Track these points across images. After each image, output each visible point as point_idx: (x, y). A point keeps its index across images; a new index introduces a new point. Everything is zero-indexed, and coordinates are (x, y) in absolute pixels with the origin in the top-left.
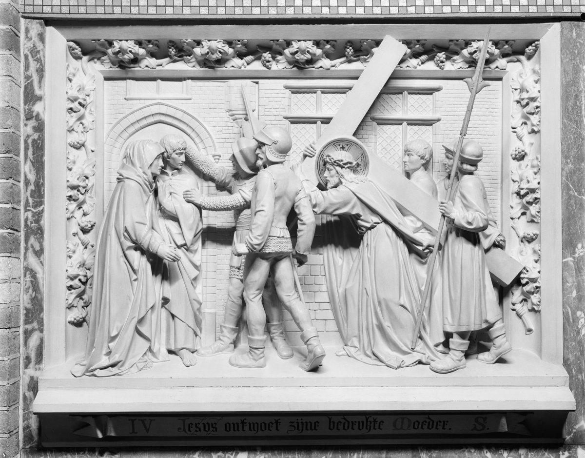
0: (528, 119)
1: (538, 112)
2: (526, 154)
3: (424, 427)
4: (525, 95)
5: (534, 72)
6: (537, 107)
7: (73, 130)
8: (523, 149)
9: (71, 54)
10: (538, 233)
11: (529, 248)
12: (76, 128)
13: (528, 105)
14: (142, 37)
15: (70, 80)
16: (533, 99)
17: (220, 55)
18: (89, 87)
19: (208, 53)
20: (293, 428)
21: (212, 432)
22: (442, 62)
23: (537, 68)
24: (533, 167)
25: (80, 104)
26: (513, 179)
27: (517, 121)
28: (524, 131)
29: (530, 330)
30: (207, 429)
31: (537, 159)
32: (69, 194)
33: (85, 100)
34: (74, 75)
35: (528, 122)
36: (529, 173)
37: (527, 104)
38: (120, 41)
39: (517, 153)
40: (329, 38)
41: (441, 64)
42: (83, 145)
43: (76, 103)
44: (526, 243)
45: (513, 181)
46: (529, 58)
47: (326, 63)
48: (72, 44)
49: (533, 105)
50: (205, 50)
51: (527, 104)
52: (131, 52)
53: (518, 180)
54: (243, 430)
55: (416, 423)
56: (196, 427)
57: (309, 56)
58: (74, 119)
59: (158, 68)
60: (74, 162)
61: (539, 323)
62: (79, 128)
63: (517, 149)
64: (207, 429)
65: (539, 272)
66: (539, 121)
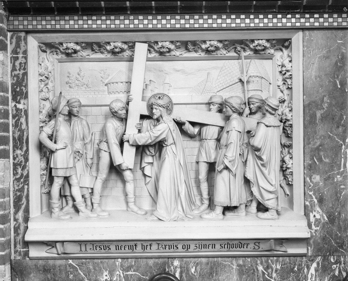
0: (286, 81)
1: (291, 77)
2: (285, 100)
3: (244, 247)
4: (284, 69)
5: (289, 56)
6: (291, 75)
7: (42, 91)
8: (284, 98)
9: (41, 50)
10: (291, 143)
11: (287, 149)
12: (44, 91)
13: (286, 75)
14: (80, 40)
15: (41, 65)
16: (288, 71)
17: (120, 50)
18: (50, 68)
19: (114, 49)
20: (196, 248)
21: (108, 251)
22: (239, 51)
23: (290, 54)
24: (288, 107)
25: (46, 77)
26: (279, 113)
27: (280, 83)
28: (284, 88)
29: (288, 195)
30: (105, 249)
31: (291, 103)
32: (41, 125)
33: (49, 75)
34: (43, 62)
35: (286, 83)
36: (287, 110)
37: (285, 73)
38: (67, 43)
39: (280, 100)
40: (177, 40)
41: (239, 53)
42: (48, 99)
43: (44, 77)
44: (285, 148)
45: (278, 114)
46: (287, 47)
47: (177, 53)
48: (41, 45)
49: (288, 74)
50: (112, 47)
51: (285, 73)
52: (72, 49)
53: (281, 115)
54: (121, 249)
55: (184, 246)
56: (99, 247)
57: (168, 50)
58: (43, 86)
59: (87, 57)
60: (43, 108)
61: (291, 190)
62: (45, 90)
63: (280, 98)
64: (105, 249)
65: (292, 164)
66: (292, 83)
